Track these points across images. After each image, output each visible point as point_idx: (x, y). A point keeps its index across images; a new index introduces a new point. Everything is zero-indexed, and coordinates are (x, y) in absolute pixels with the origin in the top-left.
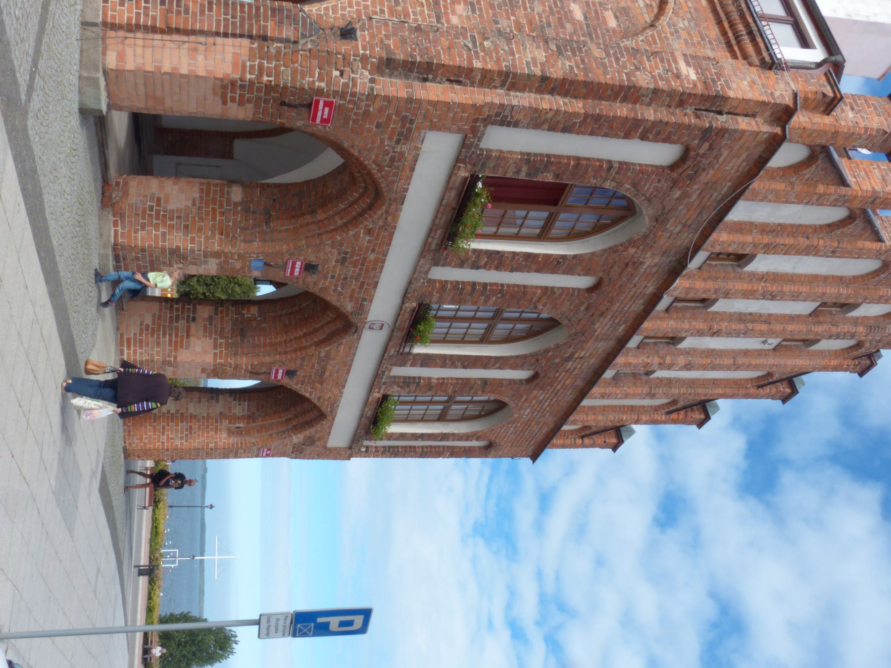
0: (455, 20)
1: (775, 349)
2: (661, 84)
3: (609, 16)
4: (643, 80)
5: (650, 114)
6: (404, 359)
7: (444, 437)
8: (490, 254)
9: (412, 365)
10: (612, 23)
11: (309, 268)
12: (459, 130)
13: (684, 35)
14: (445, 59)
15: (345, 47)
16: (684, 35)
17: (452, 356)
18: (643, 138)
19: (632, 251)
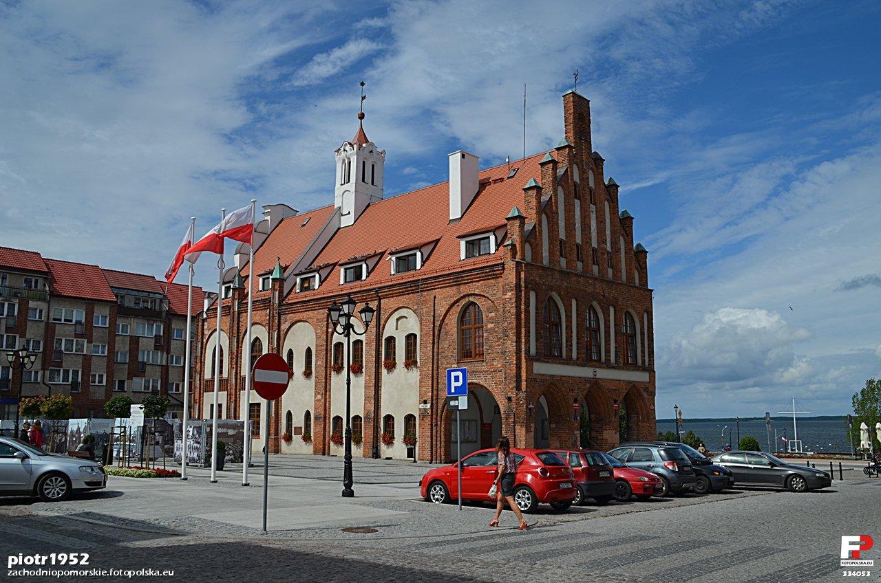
0: (499, 366)
1: (595, 205)
2: (514, 305)
3: (491, 315)
4: (513, 311)
5: (523, 307)
6: (608, 360)
7: (642, 334)
8: (567, 342)
9: (610, 356)
10: (493, 314)
11: (576, 401)
12: (532, 364)
13: (495, 292)
14: (515, 371)
15: (514, 399)
16: (495, 292)
17: (605, 342)
18: (529, 306)
19: (562, 293)
